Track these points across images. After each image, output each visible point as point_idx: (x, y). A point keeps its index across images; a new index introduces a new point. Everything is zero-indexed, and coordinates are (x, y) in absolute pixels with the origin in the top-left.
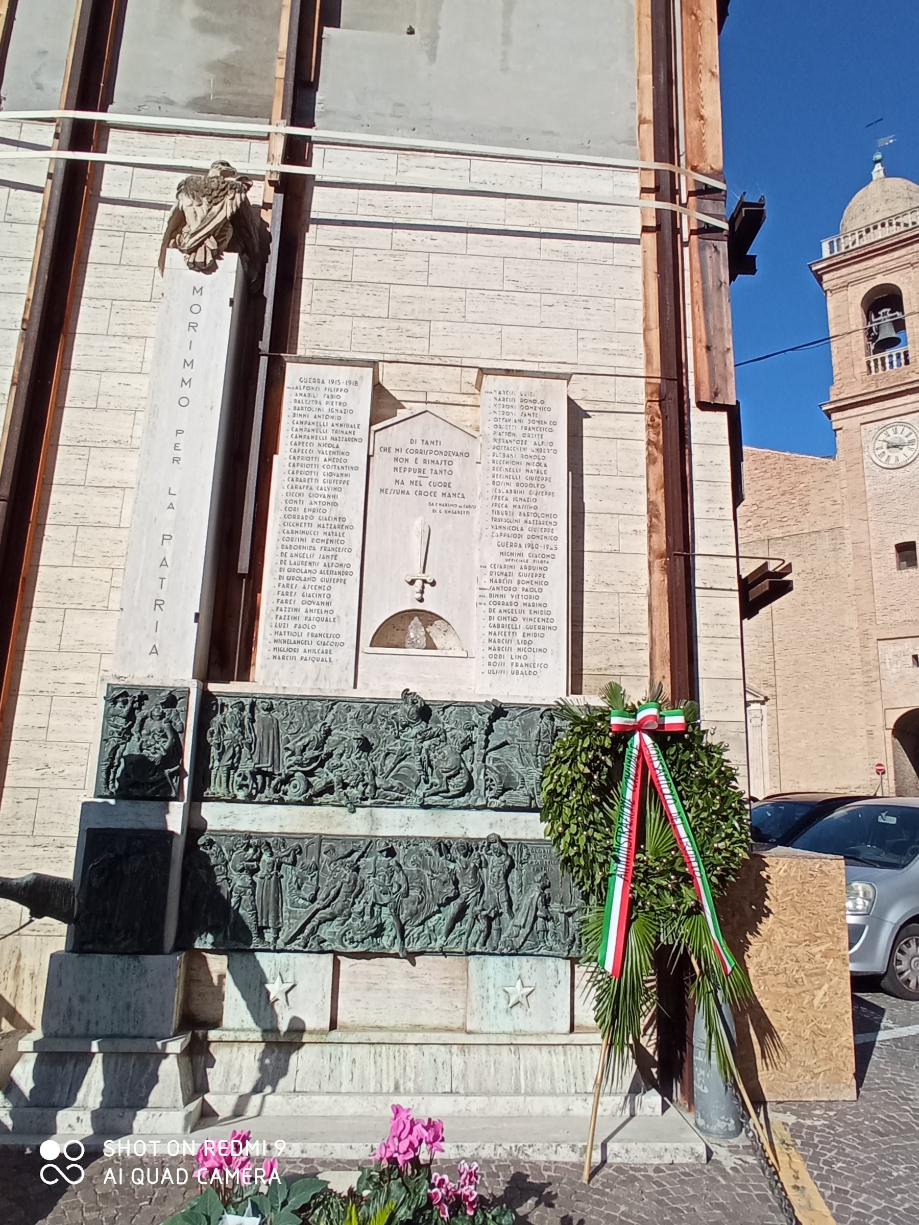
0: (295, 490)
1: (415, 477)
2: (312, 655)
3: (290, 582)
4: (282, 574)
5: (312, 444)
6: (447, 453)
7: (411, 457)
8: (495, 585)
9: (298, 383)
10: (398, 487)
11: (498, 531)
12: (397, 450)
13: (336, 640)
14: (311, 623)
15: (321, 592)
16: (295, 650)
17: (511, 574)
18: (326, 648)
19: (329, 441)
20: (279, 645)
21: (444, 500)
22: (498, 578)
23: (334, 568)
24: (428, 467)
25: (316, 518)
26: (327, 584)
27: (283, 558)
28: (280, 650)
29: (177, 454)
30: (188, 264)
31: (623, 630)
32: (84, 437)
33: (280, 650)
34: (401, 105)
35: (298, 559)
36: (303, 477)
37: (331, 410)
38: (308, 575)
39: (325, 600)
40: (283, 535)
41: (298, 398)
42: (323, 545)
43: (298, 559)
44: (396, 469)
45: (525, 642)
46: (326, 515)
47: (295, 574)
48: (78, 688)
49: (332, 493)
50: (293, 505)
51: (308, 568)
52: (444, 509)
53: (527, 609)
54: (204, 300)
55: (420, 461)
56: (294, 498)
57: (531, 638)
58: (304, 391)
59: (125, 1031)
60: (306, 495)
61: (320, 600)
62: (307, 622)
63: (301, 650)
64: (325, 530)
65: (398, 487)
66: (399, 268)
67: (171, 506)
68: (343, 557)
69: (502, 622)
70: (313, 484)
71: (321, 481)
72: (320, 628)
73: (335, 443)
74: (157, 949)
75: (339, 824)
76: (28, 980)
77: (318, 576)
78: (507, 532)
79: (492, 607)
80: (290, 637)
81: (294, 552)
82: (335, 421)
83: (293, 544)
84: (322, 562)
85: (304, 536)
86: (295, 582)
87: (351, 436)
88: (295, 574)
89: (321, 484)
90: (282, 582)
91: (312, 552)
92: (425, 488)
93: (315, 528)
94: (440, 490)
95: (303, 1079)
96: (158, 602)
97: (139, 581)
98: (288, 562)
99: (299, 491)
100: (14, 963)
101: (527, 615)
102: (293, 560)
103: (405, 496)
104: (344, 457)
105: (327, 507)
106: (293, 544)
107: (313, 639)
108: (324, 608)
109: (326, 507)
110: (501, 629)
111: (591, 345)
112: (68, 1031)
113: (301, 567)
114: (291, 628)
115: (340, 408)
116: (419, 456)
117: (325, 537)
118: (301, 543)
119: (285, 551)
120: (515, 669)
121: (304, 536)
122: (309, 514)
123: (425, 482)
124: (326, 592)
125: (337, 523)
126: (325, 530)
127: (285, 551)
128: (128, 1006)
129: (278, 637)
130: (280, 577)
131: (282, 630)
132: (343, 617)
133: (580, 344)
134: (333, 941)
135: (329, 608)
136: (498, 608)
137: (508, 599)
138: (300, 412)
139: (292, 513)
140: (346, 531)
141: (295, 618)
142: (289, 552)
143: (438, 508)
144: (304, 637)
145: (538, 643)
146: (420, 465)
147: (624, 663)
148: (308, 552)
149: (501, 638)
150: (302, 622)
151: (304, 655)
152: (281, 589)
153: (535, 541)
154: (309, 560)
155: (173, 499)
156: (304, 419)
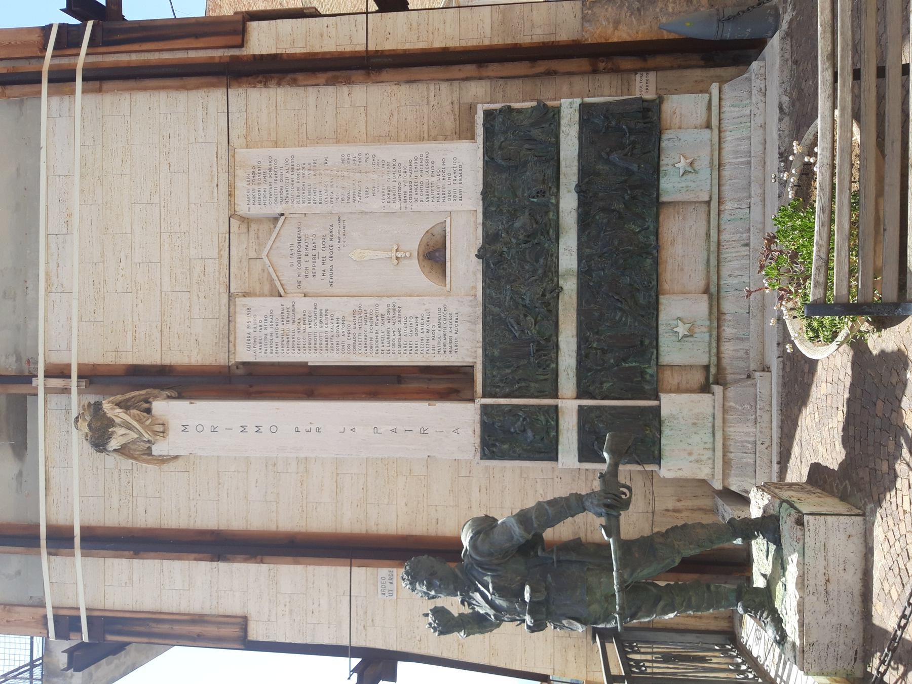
0: (335, 347)
1: (319, 262)
2: (453, 327)
3: (402, 345)
4: (397, 352)
6: (299, 238)
8: (397, 198)
10: (328, 274)
11: (357, 198)
13: (442, 310)
15: (408, 323)
18: (448, 317)
20: (448, 351)
21: (336, 240)
22: (392, 197)
24: (311, 253)
25: (355, 331)
26: (403, 320)
28: (451, 349)
31: (425, 101)
33: (451, 349)
36: (324, 343)
38: (397, 333)
39: (414, 320)
41: (263, 351)
42: (374, 325)
43: (385, 341)
46: (352, 324)
47: (397, 343)
48: (483, 490)
49: (335, 321)
50: (346, 348)
52: (342, 239)
53: (414, 175)
55: (307, 259)
56: (341, 347)
57: (435, 170)
58: (258, 347)
59: (710, 425)
60: (338, 339)
61: (414, 324)
62: (430, 332)
63: (450, 334)
64: (363, 323)
65: (328, 274)
67: (353, 430)
68: (382, 309)
71: (327, 329)
72: (434, 322)
73: (297, 321)
74: (658, 409)
75: (570, 297)
76: (683, 503)
81: (380, 345)
83: (374, 346)
85: (368, 339)
86: (402, 342)
87: (291, 310)
88: (397, 343)
89: (329, 329)
92: (327, 253)
93: (362, 331)
94: (328, 243)
95: (741, 308)
99: (335, 344)
100: (671, 513)
101: (418, 174)
102: (386, 344)
104: (307, 314)
105: (346, 323)
106: (374, 346)
108: (420, 320)
112: (711, 461)
113: (391, 339)
114: (435, 343)
115: (269, 320)
116: (302, 260)
117: (369, 324)
118: (374, 340)
119: (380, 351)
120: (458, 181)
122: (351, 336)
123: (322, 254)
124: (408, 320)
125: (357, 316)
126: (363, 323)
127: (380, 351)
128: (695, 424)
129: (442, 351)
130: (399, 352)
131: (437, 349)
133: (201, 140)
134: (650, 296)
135: (420, 317)
136: (414, 196)
137: (407, 189)
138: (274, 349)
139: (351, 348)
140: (363, 309)
142: (381, 348)
143: (342, 243)
144: (441, 333)
145: (438, 165)
146: (310, 258)
147: (450, 101)
148: (380, 335)
151: (454, 332)
152: (408, 352)
154: (386, 334)
155: (348, 429)
156: (280, 345)
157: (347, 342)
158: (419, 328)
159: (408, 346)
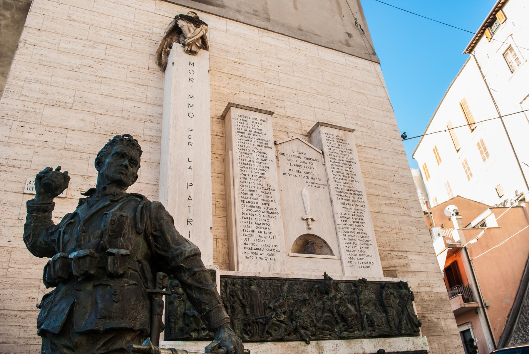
1: (298, 168)
2: (265, 256)
3: (248, 216)
4: (243, 212)
5: (248, 147)
6: (310, 159)
7: (295, 159)
8: (344, 223)
9: (238, 117)
10: (291, 172)
11: (340, 197)
12: (287, 155)
14: (262, 239)
15: (264, 222)
16: (256, 253)
17: (349, 218)
18: (271, 252)
19: (256, 146)
20: (247, 250)
21: (312, 181)
22: (344, 219)
23: (269, 210)
24: (303, 164)
25: (256, 184)
27: (243, 203)
28: (248, 253)
29: (190, 141)
30: (184, 51)
31: (392, 249)
32: (116, 131)
33: (248, 253)
34: (256, 11)
35: (250, 204)
37: (255, 132)
38: (257, 213)
39: (267, 227)
40: (241, 191)
41: (239, 124)
42: (262, 198)
43: (250, 204)
44: (288, 164)
45: (362, 251)
46: (261, 183)
49: (262, 172)
51: (256, 209)
52: (313, 185)
53: (359, 235)
54: (195, 68)
55: (299, 161)
56: (244, 173)
57: (364, 250)
58: (241, 121)
62: (260, 238)
63: (259, 254)
64: (262, 190)
65: (291, 172)
66: (266, 76)
67: (190, 168)
68: (273, 205)
69: (350, 241)
70: (252, 166)
72: (267, 242)
73: (260, 148)
77: (262, 214)
78: (343, 198)
79: (345, 234)
80: (252, 246)
82: (258, 138)
83: (247, 196)
84: (263, 207)
85: (251, 193)
86: (250, 216)
87: (267, 145)
89: (256, 167)
90: (243, 215)
91: (257, 201)
92: (303, 174)
94: (310, 176)
96: (189, 220)
97: (176, 207)
98: (245, 206)
99: (246, 169)
101: (360, 238)
102: (249, 204)
103: (295, 177)
104: (265, 155)
105: (261, 179)
106: (247, 196)
107: (264, 247)
108: (267, 231)
109: (260, 179)
110: (351, 245)
111: (351, 121)
113: (253, 209)
114: (252, 241)
115: (259, 131)
116: (297, 159)
117: (262, 194)
119: (243, 199)
120: (361, 265)
121: (251, 193)
122: (252, 181)
123: (302, 171)
124: (267, 222)
125: (266, 187)
129: (246, 246)
132: (277, 236)
133: (347, 120)
135: (270, 231)
136: (347, 234)
137: (350, 230)
138: (241, 131)
140: (271, 191)
141: (253, 236)
142: (246, 200)
143: (311, 184)
144: (259, 247)
145: (367, 252)
146: (299, 163)
147: (396, 265)
148: (255, 201)
149: (351, 249)
150: (257, 238)
151: (261, 256)
152: (244, 220)
153: (356, 203)
154: (256, 205)
156: (243, 135)
157: (248, 178)
158: (262, 230)
159: (248, 220)
